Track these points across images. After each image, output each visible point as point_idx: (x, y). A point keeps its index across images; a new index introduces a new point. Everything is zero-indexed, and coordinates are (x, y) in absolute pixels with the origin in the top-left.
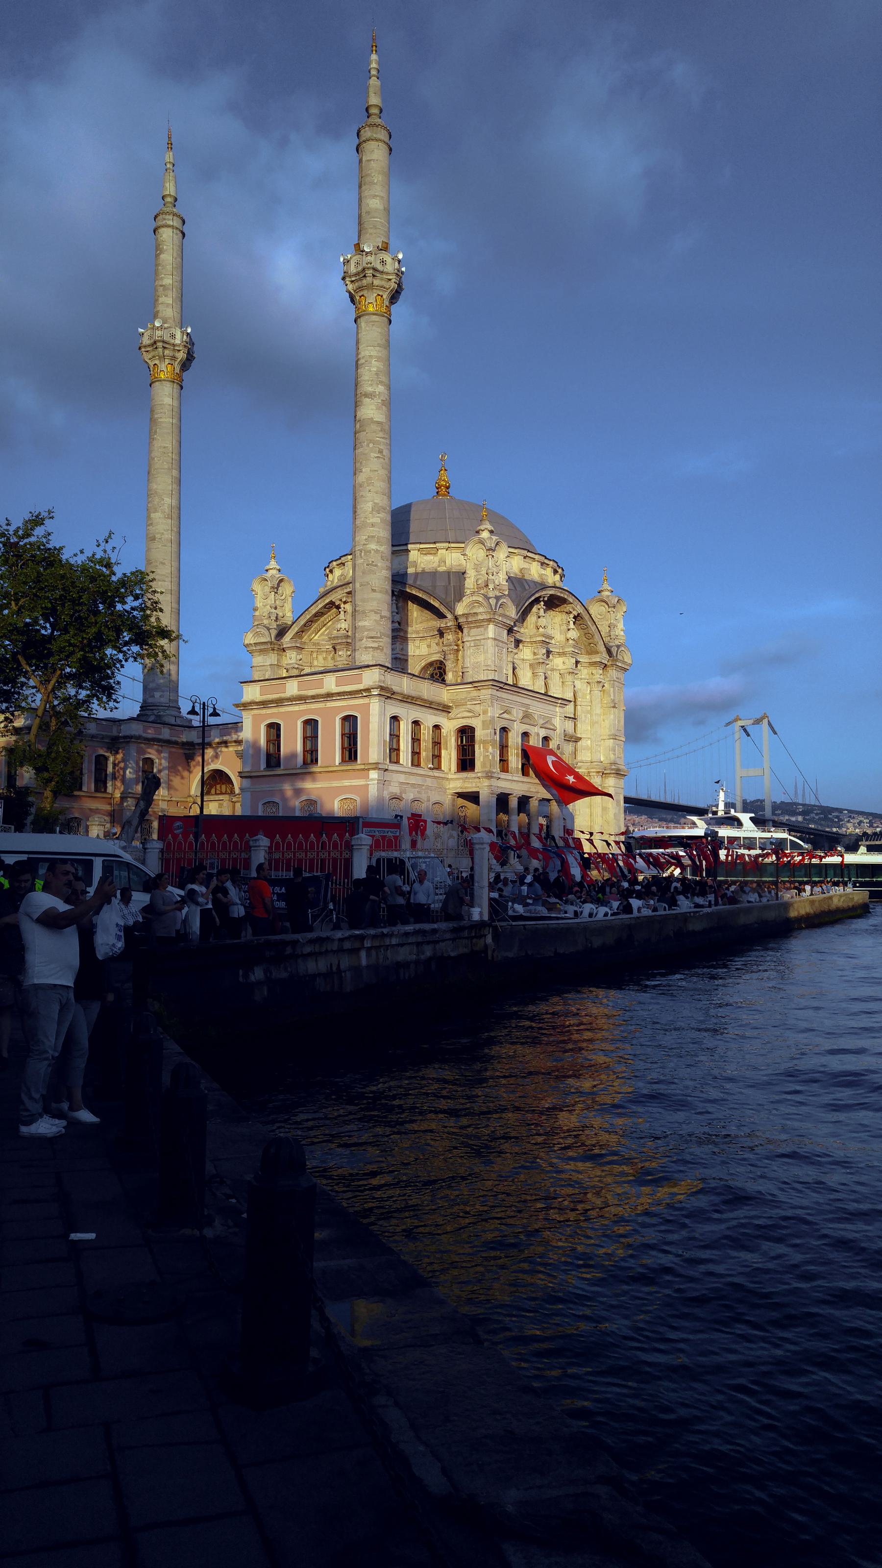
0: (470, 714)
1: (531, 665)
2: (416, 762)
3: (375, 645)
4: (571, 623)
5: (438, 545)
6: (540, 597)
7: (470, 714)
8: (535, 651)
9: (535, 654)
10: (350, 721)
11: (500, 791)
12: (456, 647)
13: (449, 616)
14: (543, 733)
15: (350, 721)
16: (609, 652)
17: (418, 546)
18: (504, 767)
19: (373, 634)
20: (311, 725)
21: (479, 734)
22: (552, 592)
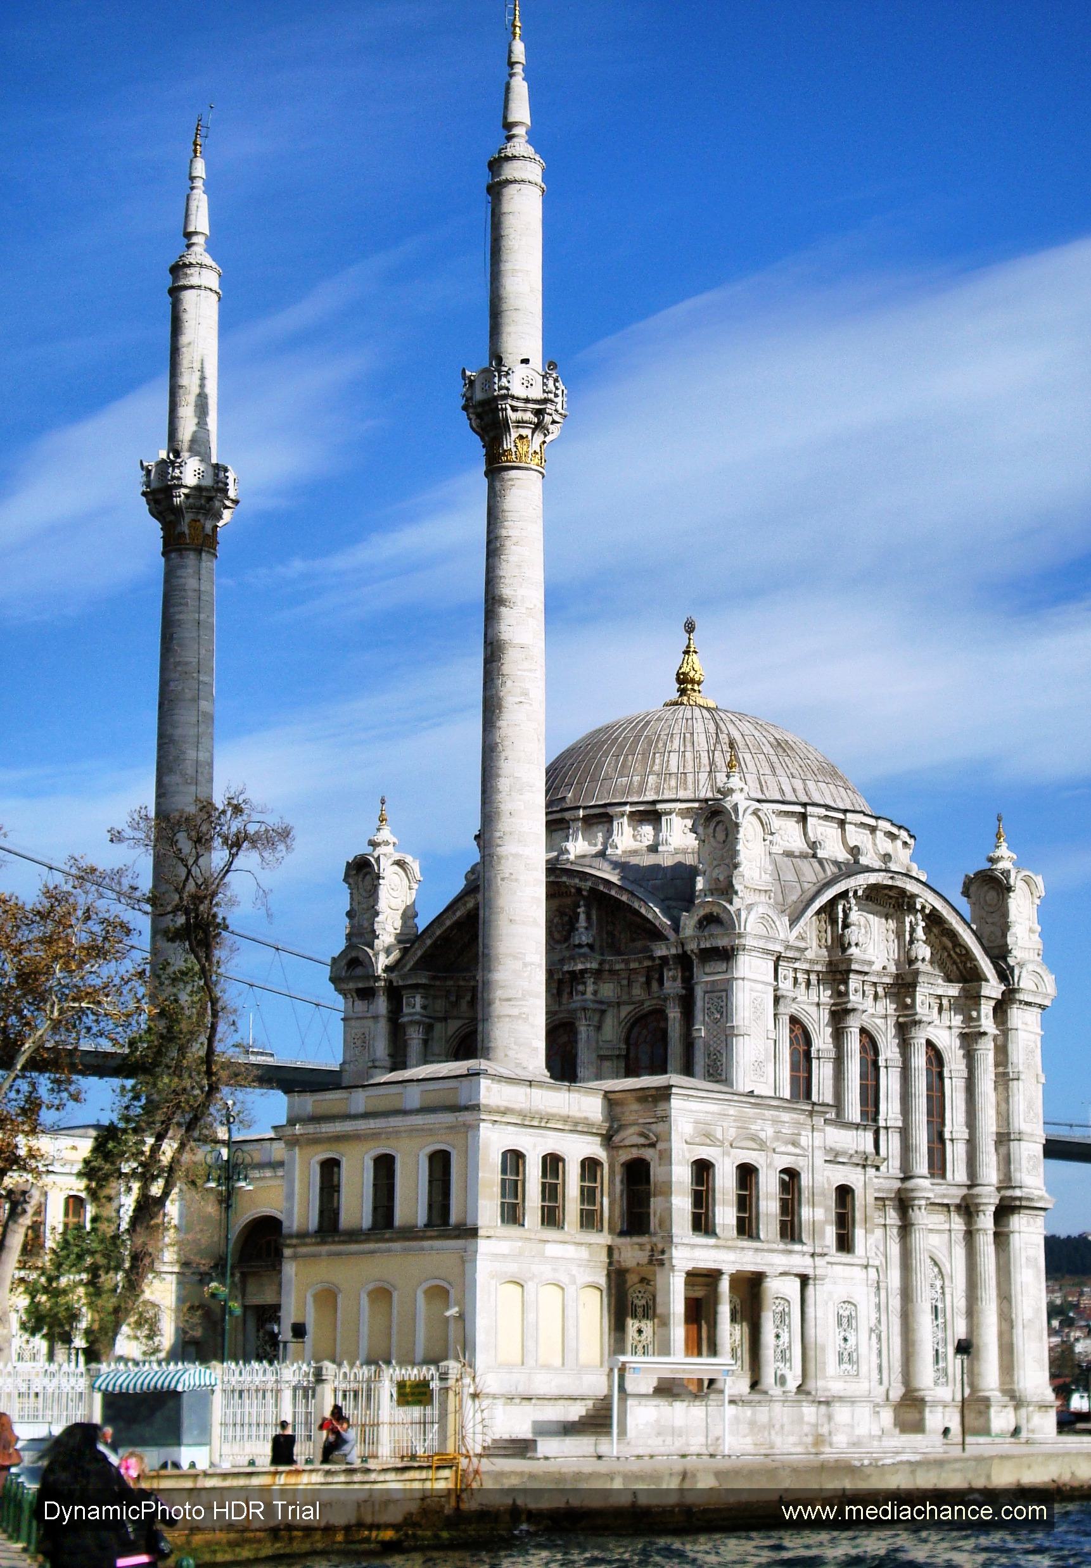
0: (642, 1141)
1: (833, 1014)
2: (551, 1217)
3: (515, 1012)
4: (920, 933)
5: (659, 807)
6: (846, 892)
7: (642, 1141)
8: (842, 988)
9: (840, 994)
10: (440, 1163)
11: (689, 1266)
12: (684, 992)
13: (671, 935)
14: (785, 1162)
15: (440, 1163)
16: (1004, 975)
17: (628, 809)
18: (702, 1223)
19: (509, 993)
20: (385, 1166)
21: (656, 1172)
22: (873, 878)
